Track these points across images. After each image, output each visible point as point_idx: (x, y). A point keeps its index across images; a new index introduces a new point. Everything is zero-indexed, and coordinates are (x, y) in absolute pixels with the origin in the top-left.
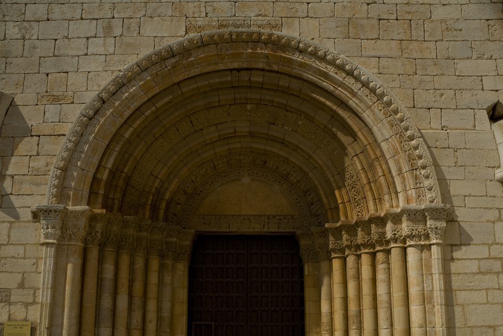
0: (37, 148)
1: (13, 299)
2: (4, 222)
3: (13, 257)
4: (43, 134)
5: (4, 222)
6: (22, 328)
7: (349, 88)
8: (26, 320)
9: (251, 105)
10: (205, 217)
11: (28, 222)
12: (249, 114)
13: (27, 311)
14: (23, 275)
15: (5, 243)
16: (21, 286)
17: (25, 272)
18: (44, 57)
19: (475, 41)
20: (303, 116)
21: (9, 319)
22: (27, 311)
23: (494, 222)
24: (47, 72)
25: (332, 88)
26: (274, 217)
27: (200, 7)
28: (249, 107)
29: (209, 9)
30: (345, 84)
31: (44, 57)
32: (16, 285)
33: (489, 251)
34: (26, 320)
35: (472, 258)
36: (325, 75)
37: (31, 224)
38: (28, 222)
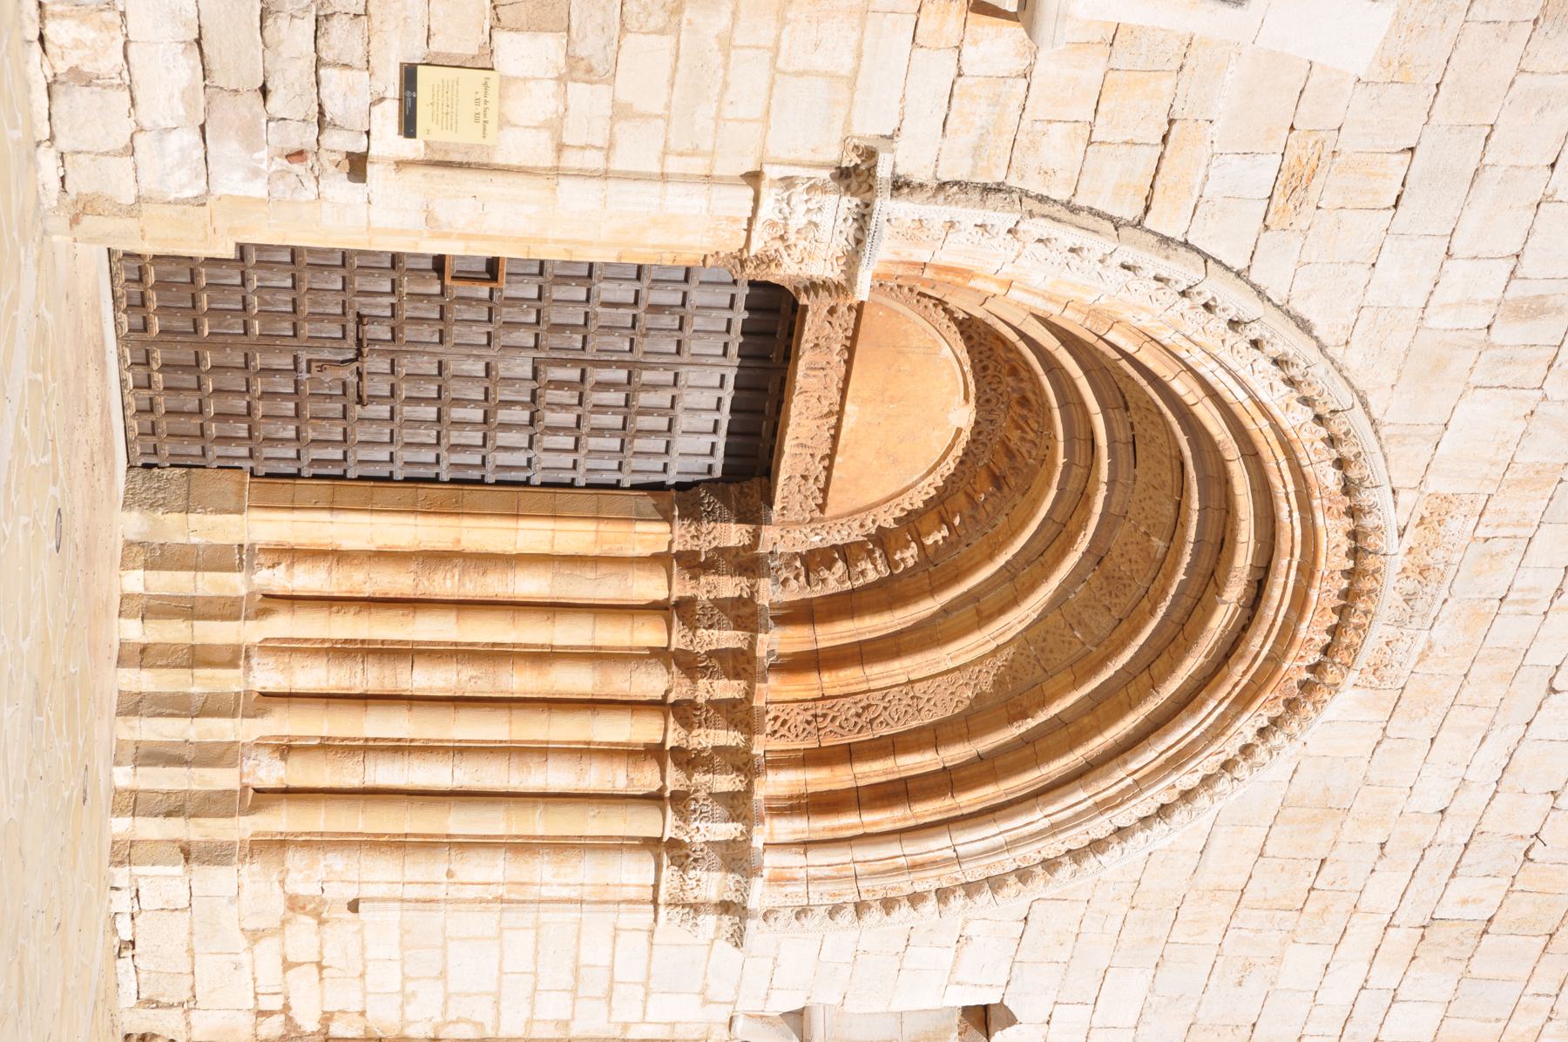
0: (1119, 139)
1: (577, 90)
2: (859, 57)
3: (726, 85)
4: (1167, 154)
5: (859, 57)
6: (477, 121)
7: (1122, 803)
8: (504, 123)
9: (1162, 550)
10: (854, 314)
11: (848, 123)
12: (1143, 529)
13: (535, 128)
14: (658, 116)
15: (781, 64)
16: (620, 112)
17: (668, 123)
18: (1487, 138)
19: (1199, 1004)
20: (1094, 649)
21: (506, 81)
22: (535, 128)
23: (702, 993)
24: (1418, 152)
25: (1133, 766)
26: (829, 469)
27: (1519, 524)
28: (1158, 544)
29: (1499, 546)
30: (1134, 796)
31: (1487, 138)
32: (624, 96)
33: (630, 983)
34: (504, 123)
35: (616, 956)
36: (1176, 761)
37: (838, 135)
38: (848, 123)
